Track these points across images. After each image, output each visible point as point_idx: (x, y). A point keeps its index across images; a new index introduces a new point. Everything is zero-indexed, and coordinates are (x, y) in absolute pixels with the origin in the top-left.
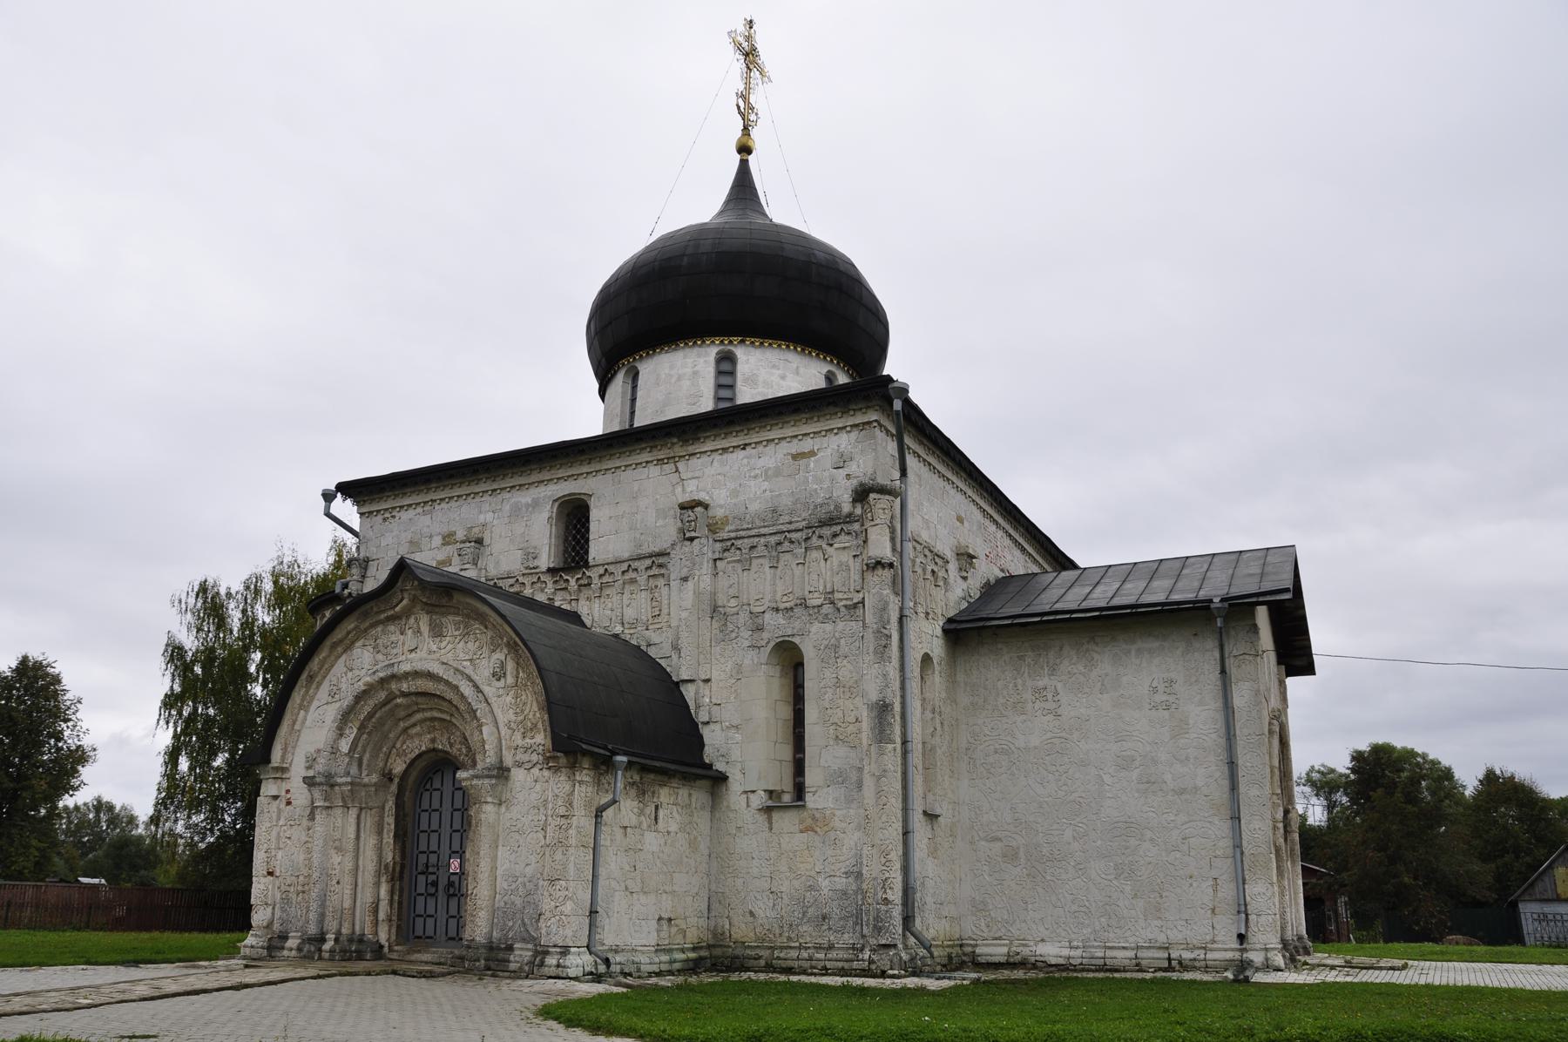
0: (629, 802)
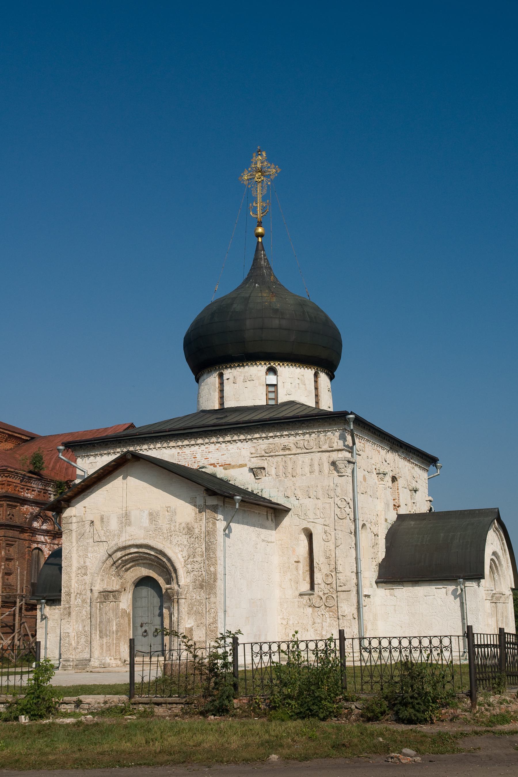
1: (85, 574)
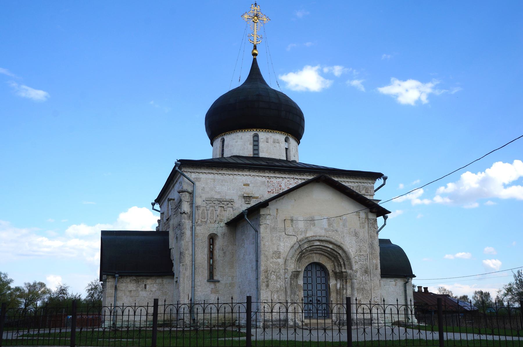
0: (132, 285)
1: (279, 257)
